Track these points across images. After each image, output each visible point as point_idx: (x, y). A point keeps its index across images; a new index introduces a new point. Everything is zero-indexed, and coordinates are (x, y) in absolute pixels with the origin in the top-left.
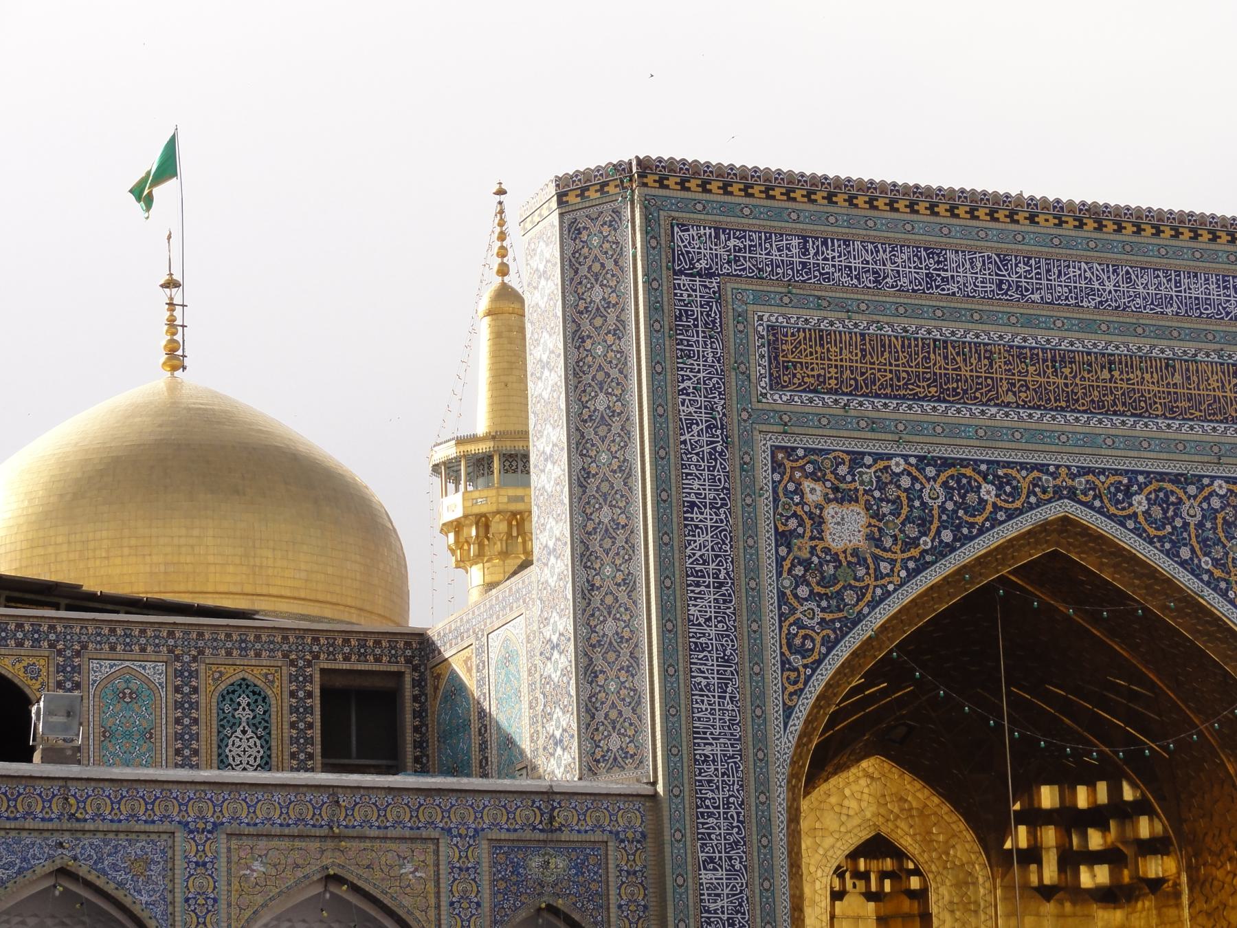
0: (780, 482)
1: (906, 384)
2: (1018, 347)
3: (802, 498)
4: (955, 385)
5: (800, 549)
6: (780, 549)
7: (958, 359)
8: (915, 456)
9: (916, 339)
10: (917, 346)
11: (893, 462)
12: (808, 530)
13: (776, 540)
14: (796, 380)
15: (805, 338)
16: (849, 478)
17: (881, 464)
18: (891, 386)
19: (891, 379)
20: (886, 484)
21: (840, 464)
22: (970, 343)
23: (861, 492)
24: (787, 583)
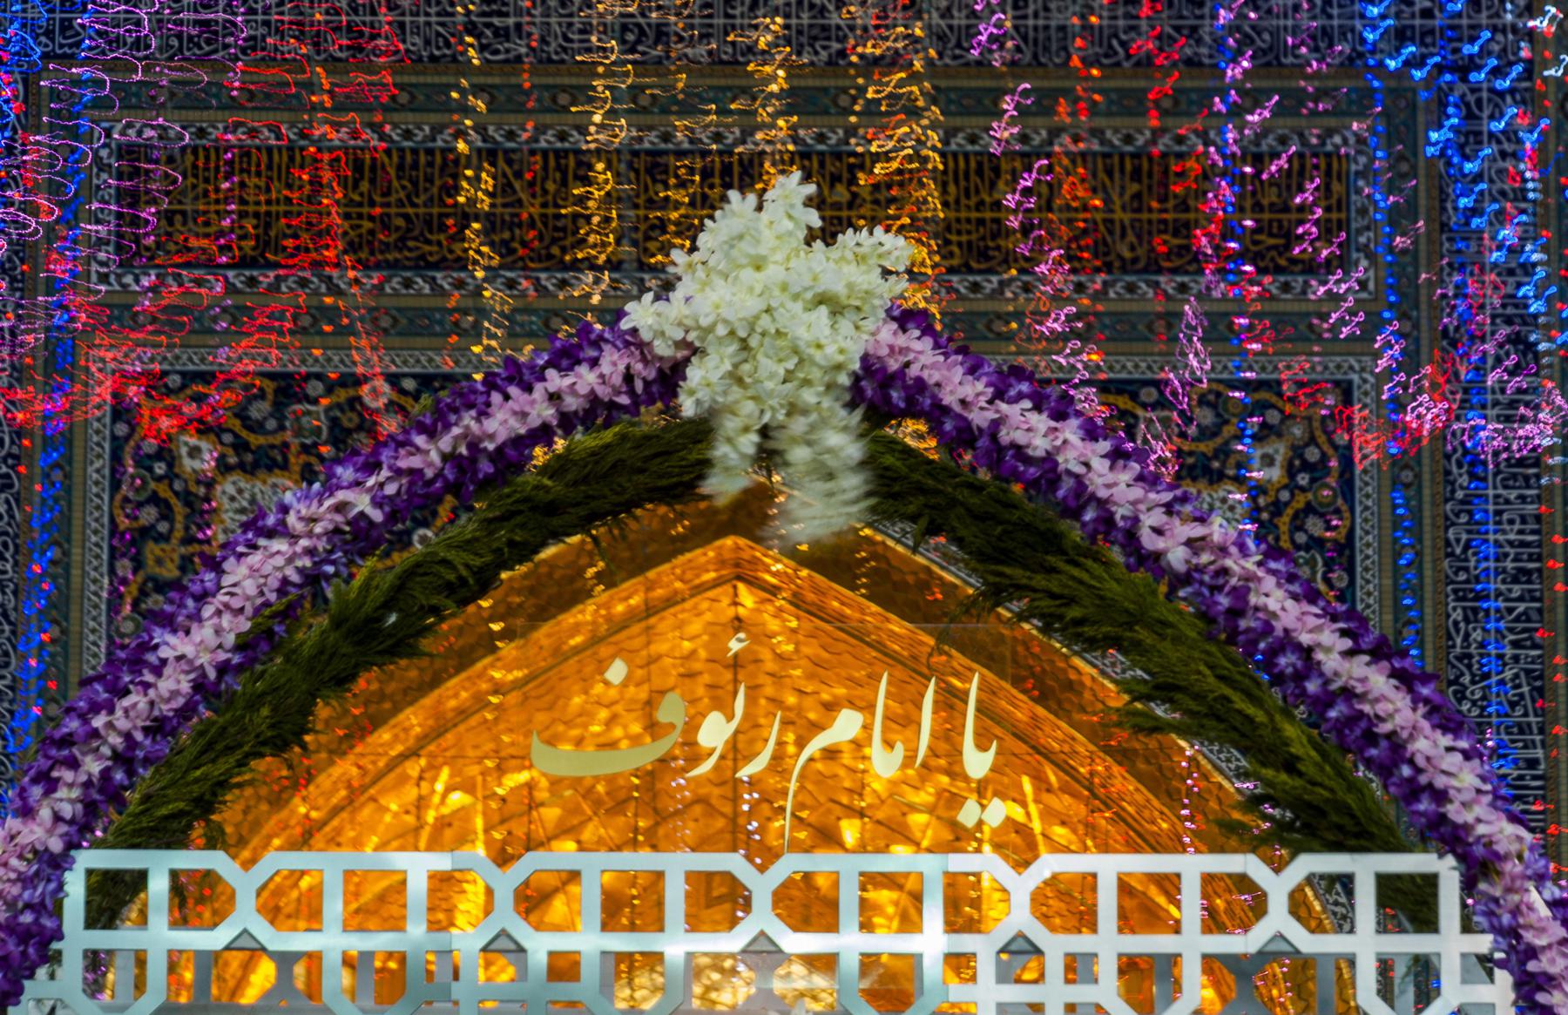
0: (127, 438)
1: (403, 239)
2: (648, 153)
3: (170, 466)
4: (506, 235)
5: (159, 562)
6: (118, 564)
7: (517, 185)
8: (414, 376)
9: (430, 152)
10: (431, 164)
11: (366, 389)
12: (179, 526)
13: (112, 549)
14: (171, 247)
15: (195, 166)
16: (271, 424)
17: (342, 395)
18: (370, 243)
19: (372, 232)
20: (349, 432)
21: (255, 397)
22: (545, 153)
23: (294, 449)
24: (128, 627)
